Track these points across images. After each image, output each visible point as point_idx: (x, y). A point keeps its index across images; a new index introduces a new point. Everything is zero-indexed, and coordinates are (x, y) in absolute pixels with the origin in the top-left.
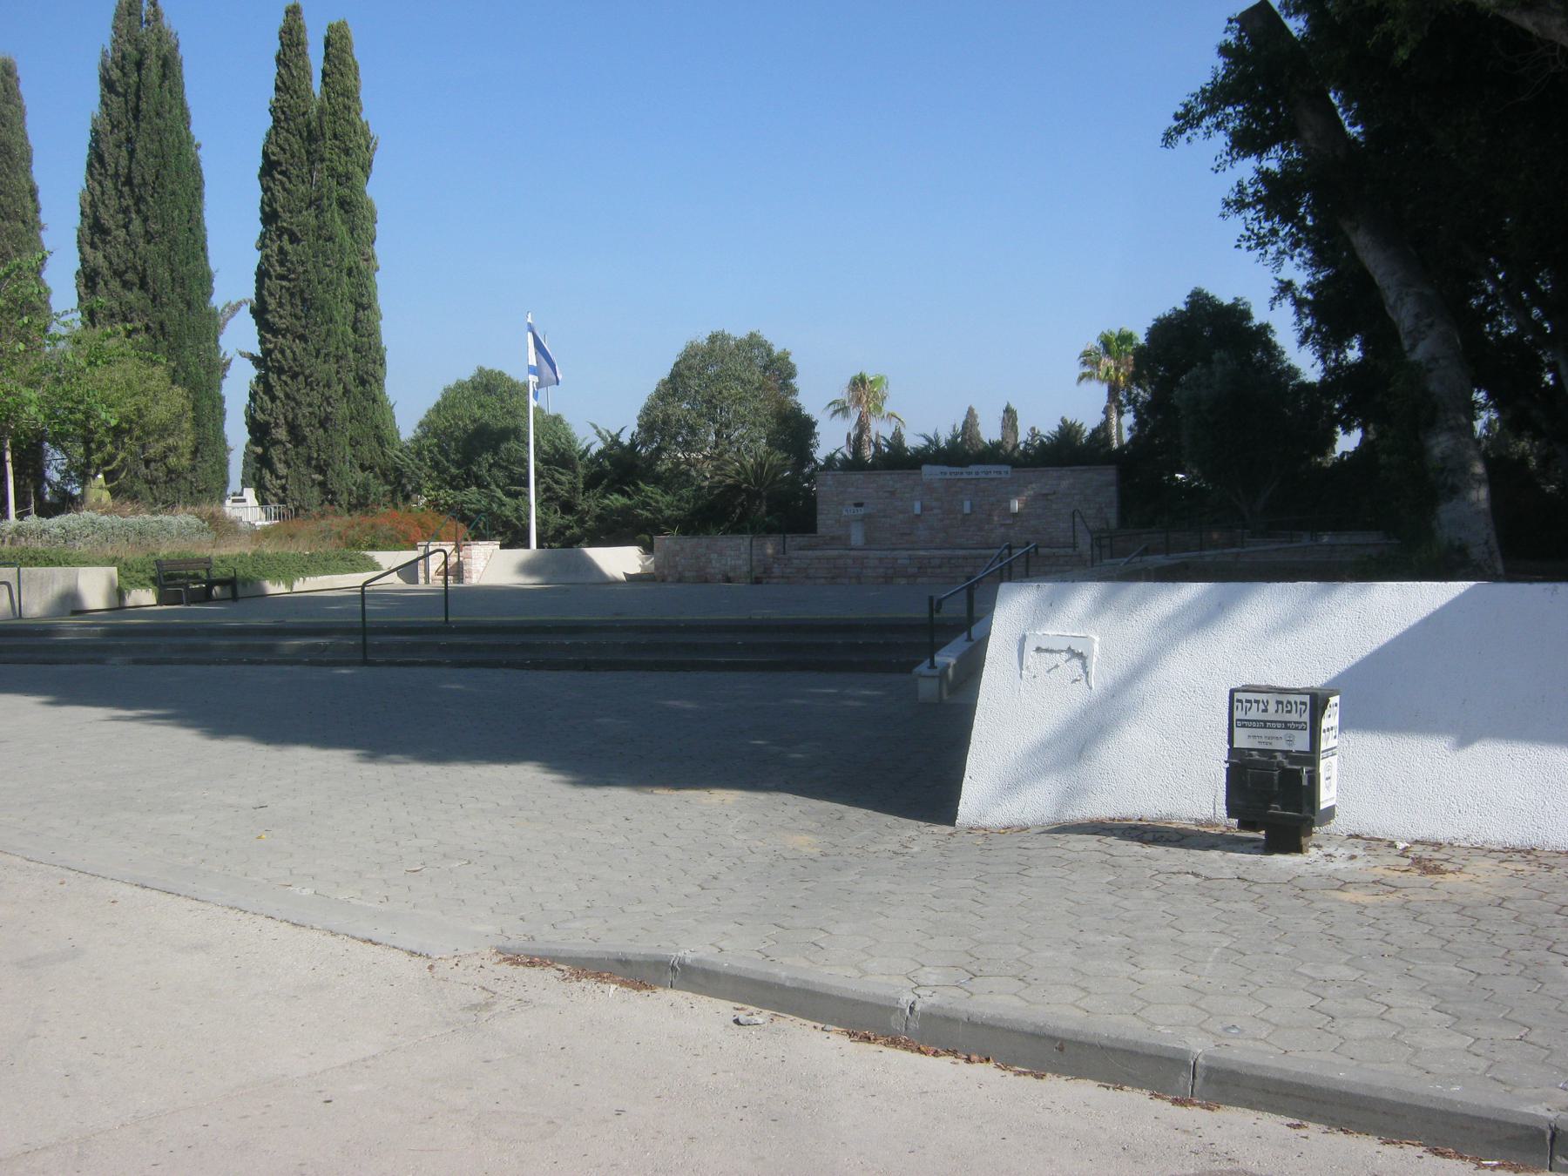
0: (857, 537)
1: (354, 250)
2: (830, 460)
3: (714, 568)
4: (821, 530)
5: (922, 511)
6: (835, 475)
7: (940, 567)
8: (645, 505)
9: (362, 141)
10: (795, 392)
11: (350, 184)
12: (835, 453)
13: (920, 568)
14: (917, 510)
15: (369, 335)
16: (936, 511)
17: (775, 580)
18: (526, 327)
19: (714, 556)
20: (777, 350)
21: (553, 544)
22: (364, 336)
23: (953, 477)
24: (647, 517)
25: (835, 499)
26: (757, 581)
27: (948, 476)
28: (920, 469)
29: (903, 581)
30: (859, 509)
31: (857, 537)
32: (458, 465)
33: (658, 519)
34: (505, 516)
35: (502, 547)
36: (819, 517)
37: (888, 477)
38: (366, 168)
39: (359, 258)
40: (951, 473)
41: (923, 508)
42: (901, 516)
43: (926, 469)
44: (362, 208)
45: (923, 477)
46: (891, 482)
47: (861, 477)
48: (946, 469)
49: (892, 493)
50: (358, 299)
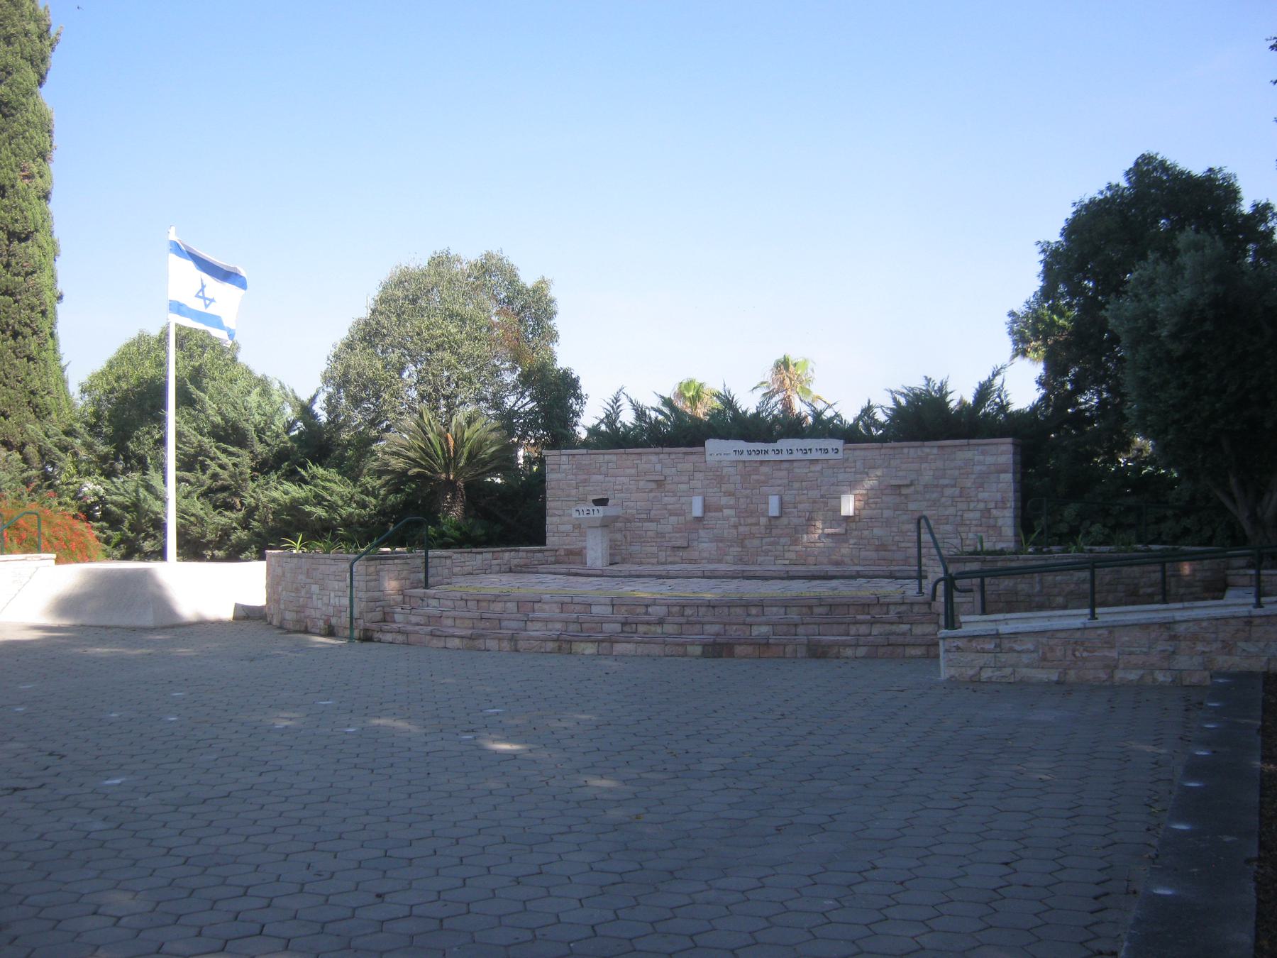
0: (596, 552)
1: (11, 164)
2: (593, 431)
3: (315, 609)
4: (551, 540)
5: (704, 512)
6: (574, 455)
7: (661, 622)
8: (319, 500)
9: (32, 27)
10: (553, 336)
11: (9, 80)
12: (598, 424)
13: (624, 624)
14: (697, 511)
15: (27, 274)
16: (727, 512)
17: (389, 637)
18: (167, 247)
19: (315, 588)
20: (528, 279)
21: (216, 552)
22: (18, 275)
23: (754, 457)
24: (320, 518)
25: (574, 492)
26: (367, 638)
27: (745, 457)
28: (704, 445)
29: (590, 649)
30: (601, 508)
31: (596, 552)
32: (109, 440)
33: (335, 519)
34: (152, 512)
35: (58, 561)
36: (549, 520)
37: (654, 458)
38: (38, 63)
39: (18, 174)
40: (749, 453)
41: (706, 508)
42: (673, 519)
43: (712, 445)
44: (27, 111)
45: (709, 458)
46: (658, 467)
47: (613, 458)
48: (741, 445)
49: (659, 483)
50: (10, 226)
